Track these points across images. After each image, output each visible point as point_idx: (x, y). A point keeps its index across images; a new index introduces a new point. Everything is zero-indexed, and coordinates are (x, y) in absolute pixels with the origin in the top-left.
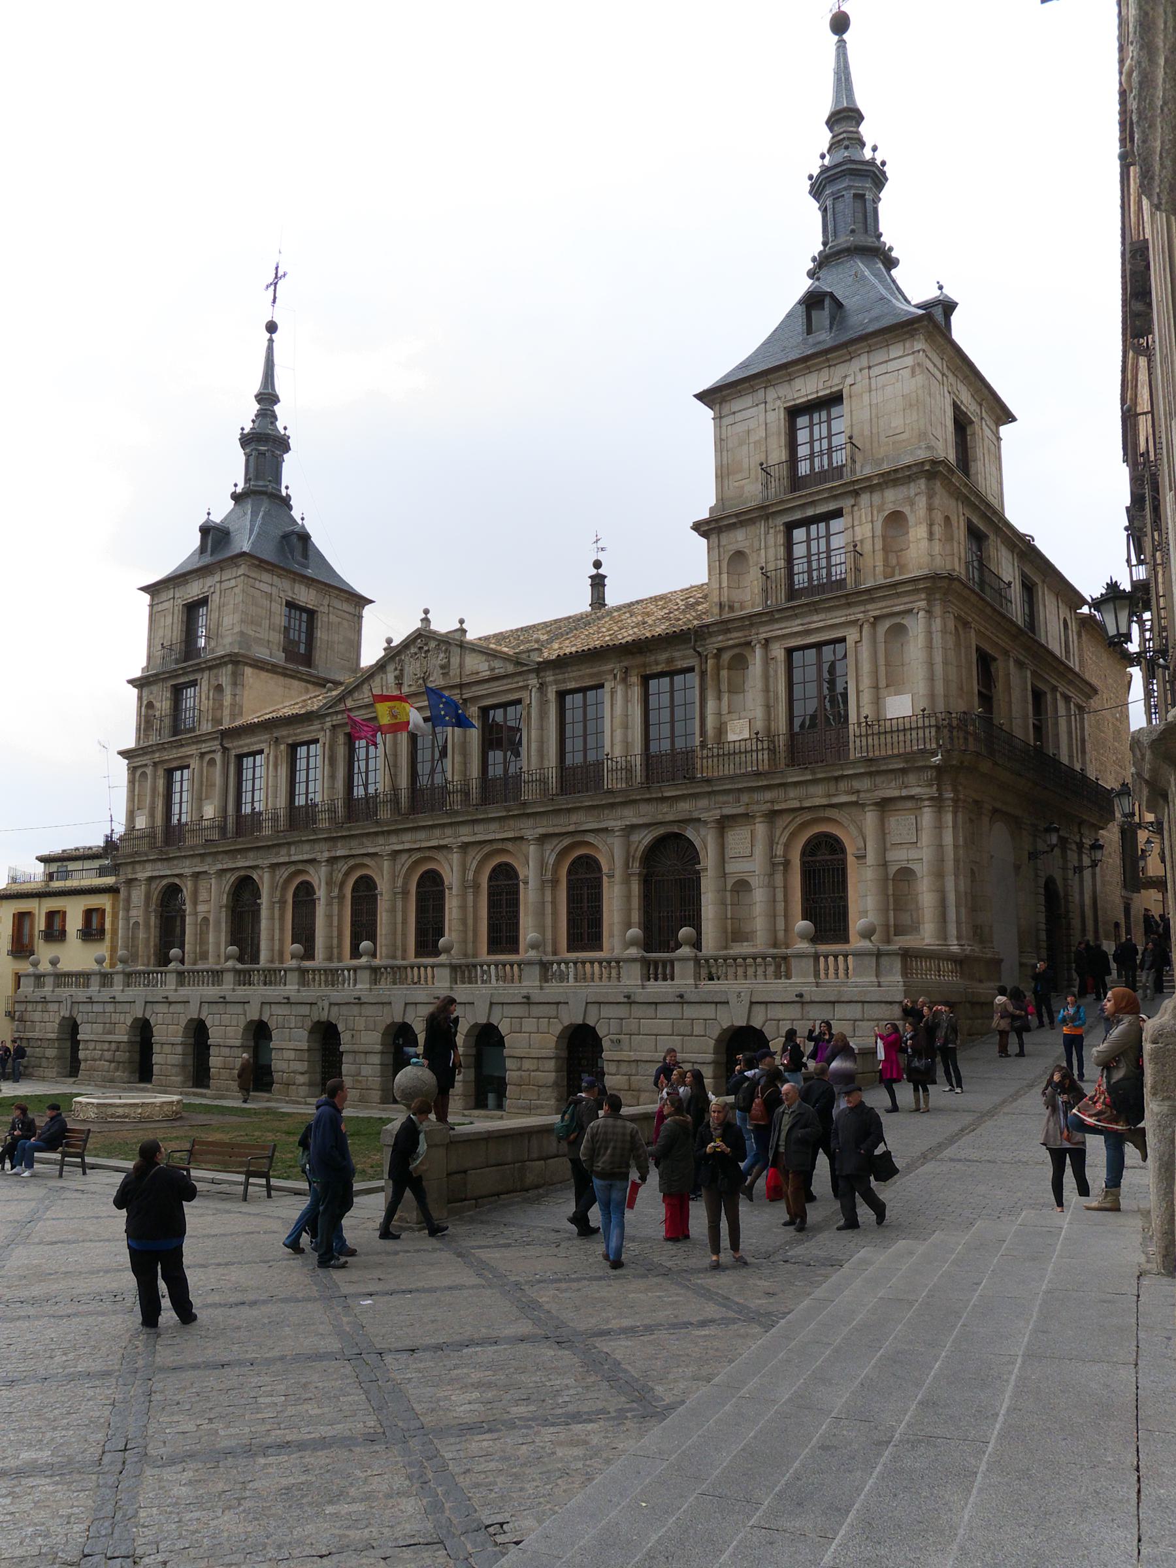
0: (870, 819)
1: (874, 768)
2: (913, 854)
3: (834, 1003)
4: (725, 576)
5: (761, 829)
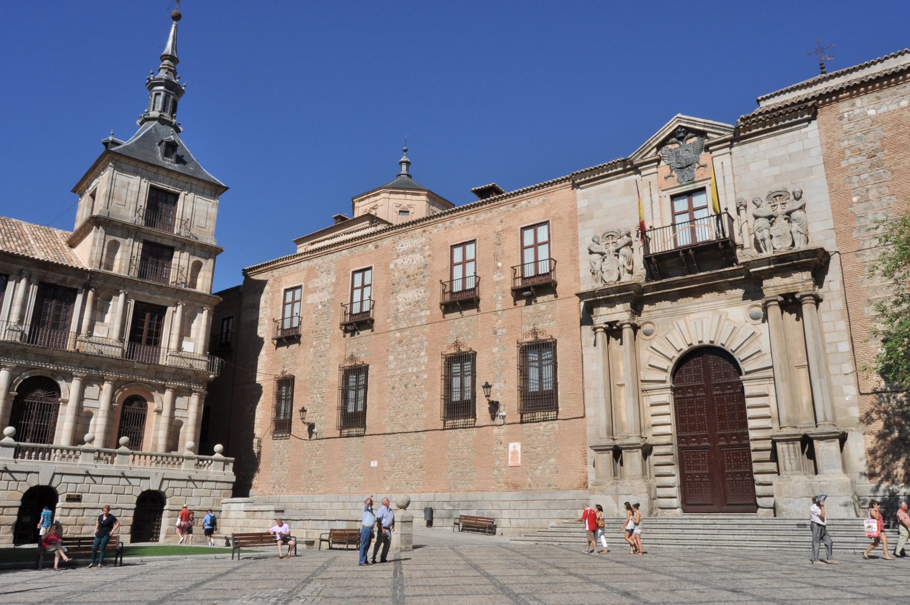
0: (168, 394)
1: (178, 373)
2: (184, 414)
3: (203, 481)
4: (105, 250)
5: (107, 386)
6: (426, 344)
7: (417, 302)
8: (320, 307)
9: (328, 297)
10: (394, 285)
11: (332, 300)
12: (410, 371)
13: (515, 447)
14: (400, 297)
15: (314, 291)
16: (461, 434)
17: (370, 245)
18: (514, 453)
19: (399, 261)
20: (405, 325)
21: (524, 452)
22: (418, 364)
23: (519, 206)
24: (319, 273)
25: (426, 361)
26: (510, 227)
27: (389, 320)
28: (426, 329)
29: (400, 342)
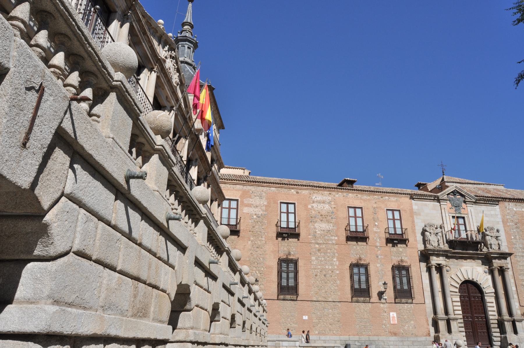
6: (336, 255)
7: (329, 231)
8: (255, 217)
9: (262, 212)
10: (312, 217)
11: (265, 215)
12: (327, 267)
13: (393, 314)
14: (316, 225)
15: (249, 205)
16: (362, 305)
17: (293, 191)
18: (393, 317)
19: (315, 205)
20: (321, 242)
21: (398, 317)
22: (332, 265)
23: (384, 198)
24: (253, 196)
25: (337, 263)
26: (380, 207)
27: (309, 237)
28: (336, 247)
29: (319, 250)
